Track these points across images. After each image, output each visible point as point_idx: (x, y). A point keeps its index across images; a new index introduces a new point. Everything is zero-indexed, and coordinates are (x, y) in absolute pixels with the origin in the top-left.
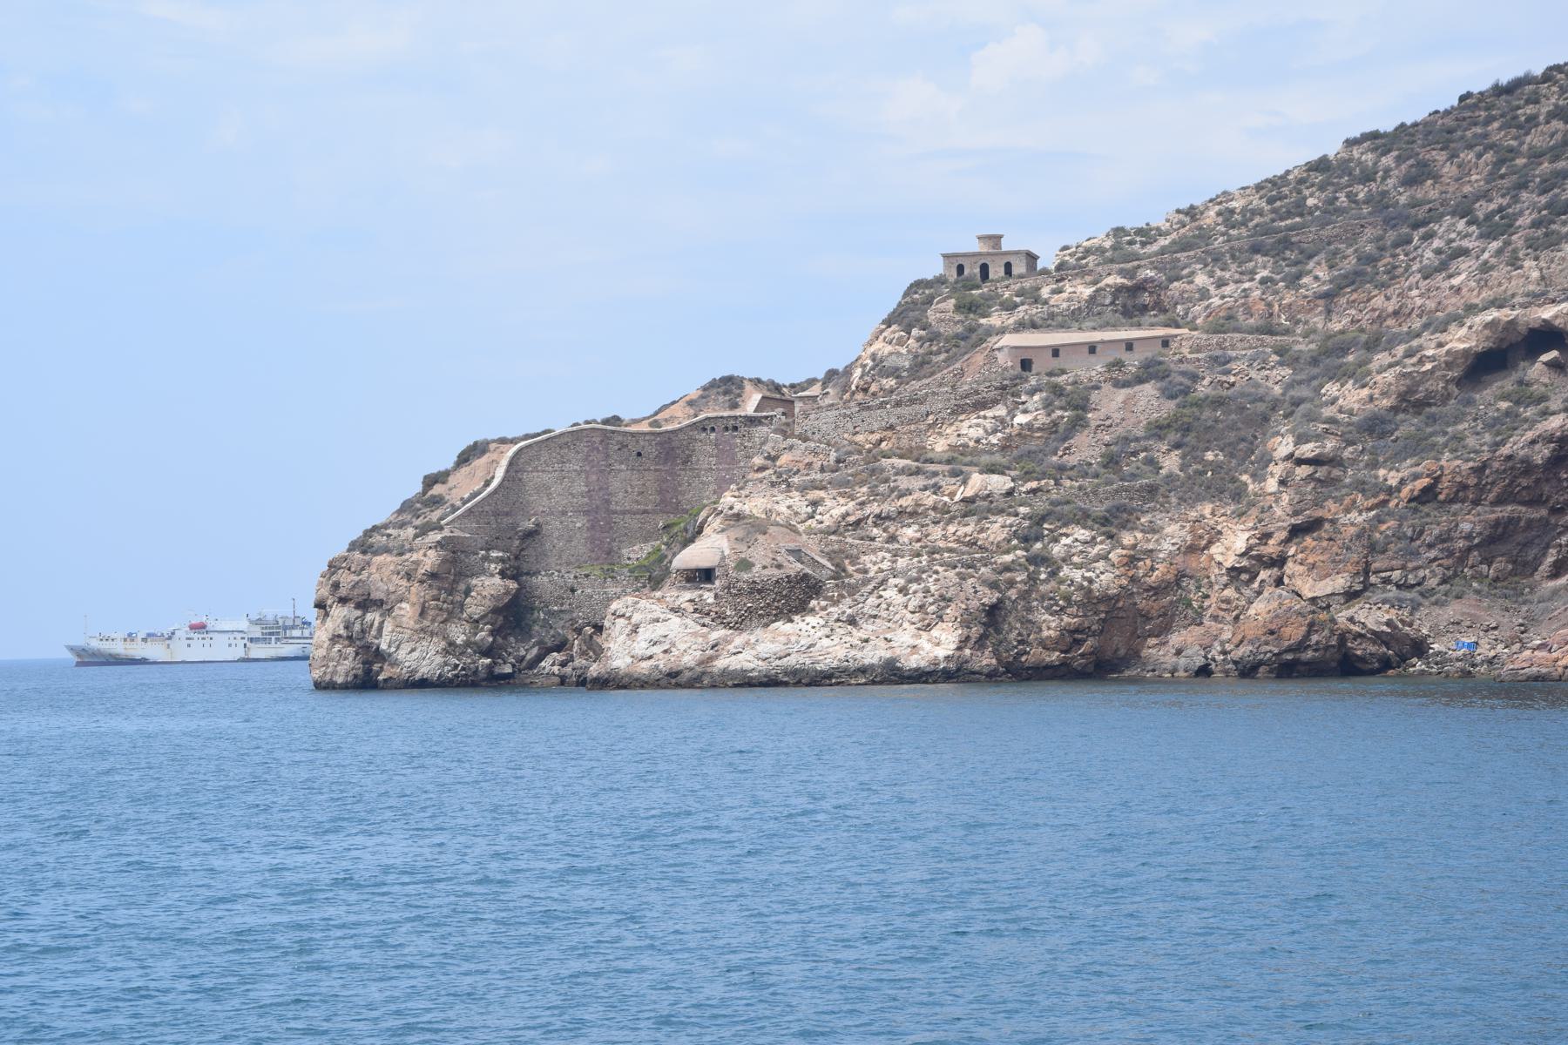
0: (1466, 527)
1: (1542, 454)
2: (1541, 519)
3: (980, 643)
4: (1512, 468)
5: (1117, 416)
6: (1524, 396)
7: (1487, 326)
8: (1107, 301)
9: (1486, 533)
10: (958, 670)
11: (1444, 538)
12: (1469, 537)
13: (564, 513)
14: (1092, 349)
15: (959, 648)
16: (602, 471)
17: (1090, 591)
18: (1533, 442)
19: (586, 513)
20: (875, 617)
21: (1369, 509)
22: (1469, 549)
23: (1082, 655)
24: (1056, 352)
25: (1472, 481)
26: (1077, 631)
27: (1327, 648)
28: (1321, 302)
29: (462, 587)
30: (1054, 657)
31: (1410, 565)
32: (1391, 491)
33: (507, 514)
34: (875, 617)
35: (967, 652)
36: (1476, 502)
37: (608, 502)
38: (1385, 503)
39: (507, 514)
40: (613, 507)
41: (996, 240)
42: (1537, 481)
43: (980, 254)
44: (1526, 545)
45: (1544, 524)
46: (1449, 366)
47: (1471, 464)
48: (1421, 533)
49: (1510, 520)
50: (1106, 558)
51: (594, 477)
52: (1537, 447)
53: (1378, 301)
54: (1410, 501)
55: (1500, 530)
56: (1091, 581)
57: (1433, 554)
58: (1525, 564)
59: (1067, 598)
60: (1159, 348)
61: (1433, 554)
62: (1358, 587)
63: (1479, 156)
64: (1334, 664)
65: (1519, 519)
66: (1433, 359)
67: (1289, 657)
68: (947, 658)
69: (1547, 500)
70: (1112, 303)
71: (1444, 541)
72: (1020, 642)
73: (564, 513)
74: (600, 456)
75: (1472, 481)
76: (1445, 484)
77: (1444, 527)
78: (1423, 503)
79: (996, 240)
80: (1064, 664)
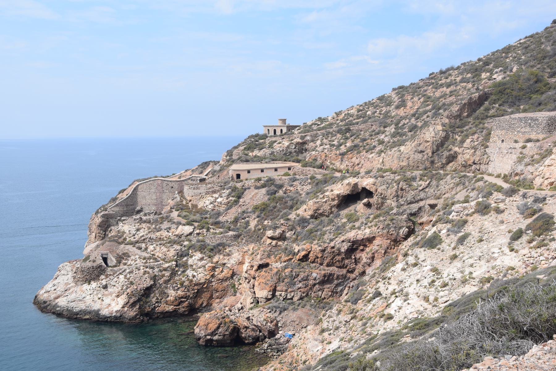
0: (314, 275)
1: (345, 247)
2: (342, 275)
3: (133, 305)
4: (333, 252)
5: (247, 201)
6: (352, 218)
7: (349, 184)
8: (293, 147)
9: (321, 279)
10: (121, 316)
11: (306, 279)
12: (315, 279)
13: (149, 205)
14: (276, 170)
15: (123, 307)
16: (160, 192)
17: (192, 281)
18: (343, 241)
19: (156, 205)
20: (114, 286)
21: (285, 262)
22: (314, 285)
23: (183, 307)
24: (249, 172)
25: (320, 255)
26: (182, 298)
27: (224, 335)
28: (340, 157)
29: (109, 229)
30: (170, 308)
31: (290, 290)
32: (295, 254)
33: (132, 205)
34: (114, 286)
35: (126, 309)
36: (321, 264)
37: (162, 202)
38: (291, 259)
39: (132, 205)
40: (163, 204)
41: (284, 121)
42: (343, 259)
43: (280, 126)
44: (338, 285)
45: (344, 277)
46: (333, 200)
47: (320, 248)
48: (298, 275)
49: (330, 275)
50: (204, 266)
51: (158, 194)
52: (345, 243)
53: (354, 160)
54: (299, 260)
55: (326, 278)
56: (194, 276)
57: (300, 285)
58: (337, 293)
59: (182, 284)
60: (287, 170)
61: (300, 285)
62: (270, 297)
63: (419, 99)
64: (228, 341)
65: (334, 274)
66: (328, 197)
67: (209, 337)
68: (117, 312)
69: (346, 267)
70: (295, 148)
71: (304, 280)
72: (156, 302)
73: (149, 205)
74: (161, 188)
75: (320, 255)
76: (311, 255)
77: (306, 274)
78: (303, 262)
79: (284, 121)
80: (175, 311)
